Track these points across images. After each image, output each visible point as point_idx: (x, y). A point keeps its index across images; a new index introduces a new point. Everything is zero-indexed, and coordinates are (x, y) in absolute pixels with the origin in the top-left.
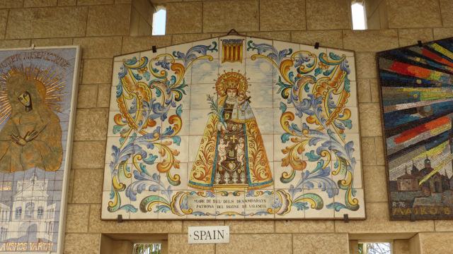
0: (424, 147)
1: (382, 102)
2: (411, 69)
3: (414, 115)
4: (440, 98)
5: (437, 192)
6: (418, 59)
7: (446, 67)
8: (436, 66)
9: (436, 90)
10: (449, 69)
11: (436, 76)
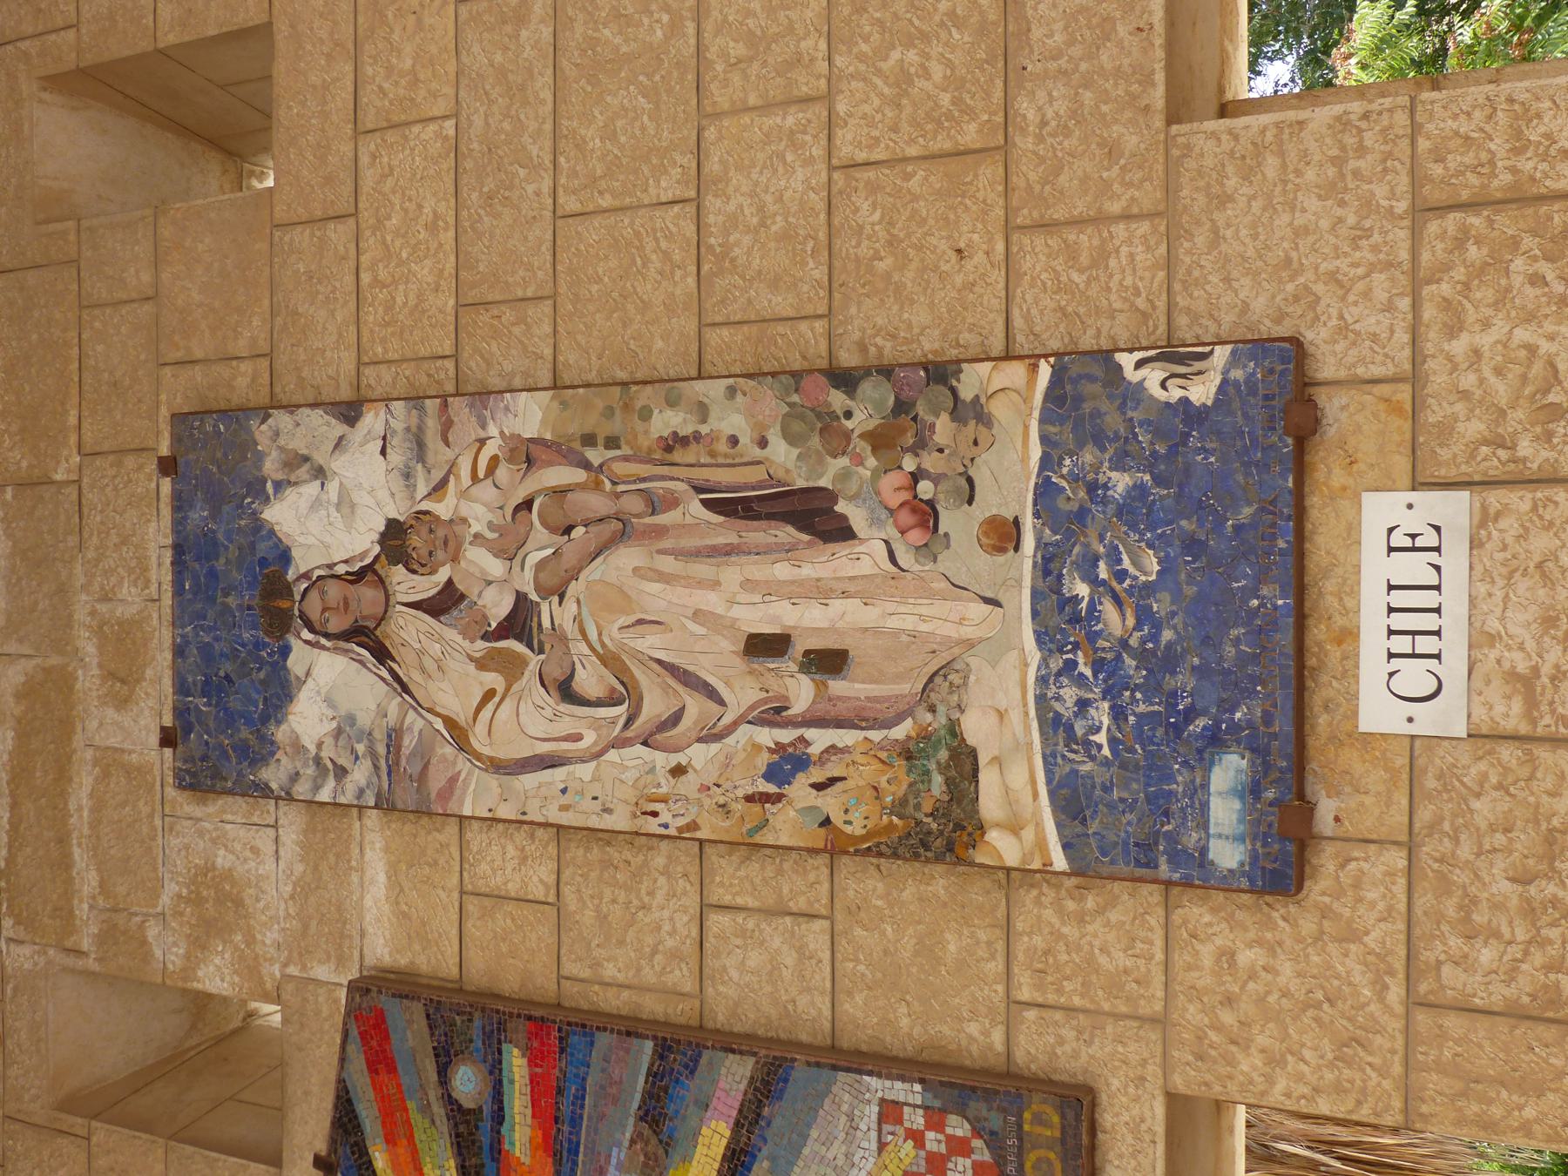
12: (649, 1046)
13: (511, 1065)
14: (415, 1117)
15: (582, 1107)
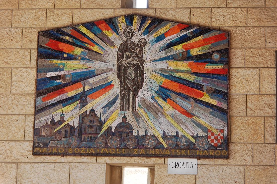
0: (61, 105)
1: (38, 71)
2: (61, 46)
3: (58, 81)
4: (79, 69)
5: (66, 137)
6: (67, 38)
7: (86, 45)
8: (79, 43)
9: (76, 62)
10: (89, 46)
11: (78, 51)
12: (227, 91)
13: (220, 65)
14: (208, 46)
15: (215, 79)
